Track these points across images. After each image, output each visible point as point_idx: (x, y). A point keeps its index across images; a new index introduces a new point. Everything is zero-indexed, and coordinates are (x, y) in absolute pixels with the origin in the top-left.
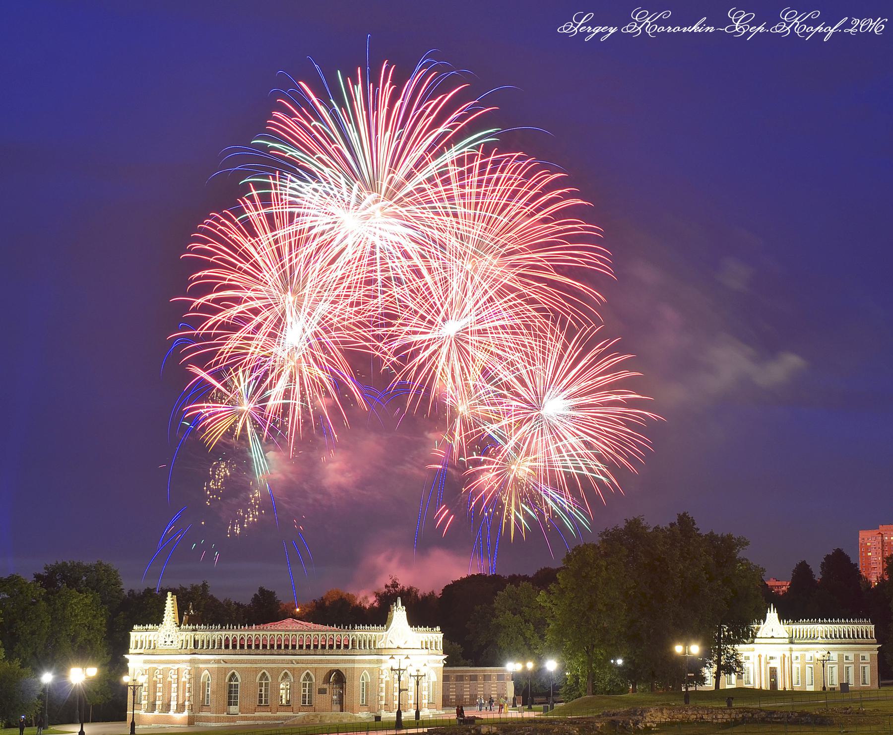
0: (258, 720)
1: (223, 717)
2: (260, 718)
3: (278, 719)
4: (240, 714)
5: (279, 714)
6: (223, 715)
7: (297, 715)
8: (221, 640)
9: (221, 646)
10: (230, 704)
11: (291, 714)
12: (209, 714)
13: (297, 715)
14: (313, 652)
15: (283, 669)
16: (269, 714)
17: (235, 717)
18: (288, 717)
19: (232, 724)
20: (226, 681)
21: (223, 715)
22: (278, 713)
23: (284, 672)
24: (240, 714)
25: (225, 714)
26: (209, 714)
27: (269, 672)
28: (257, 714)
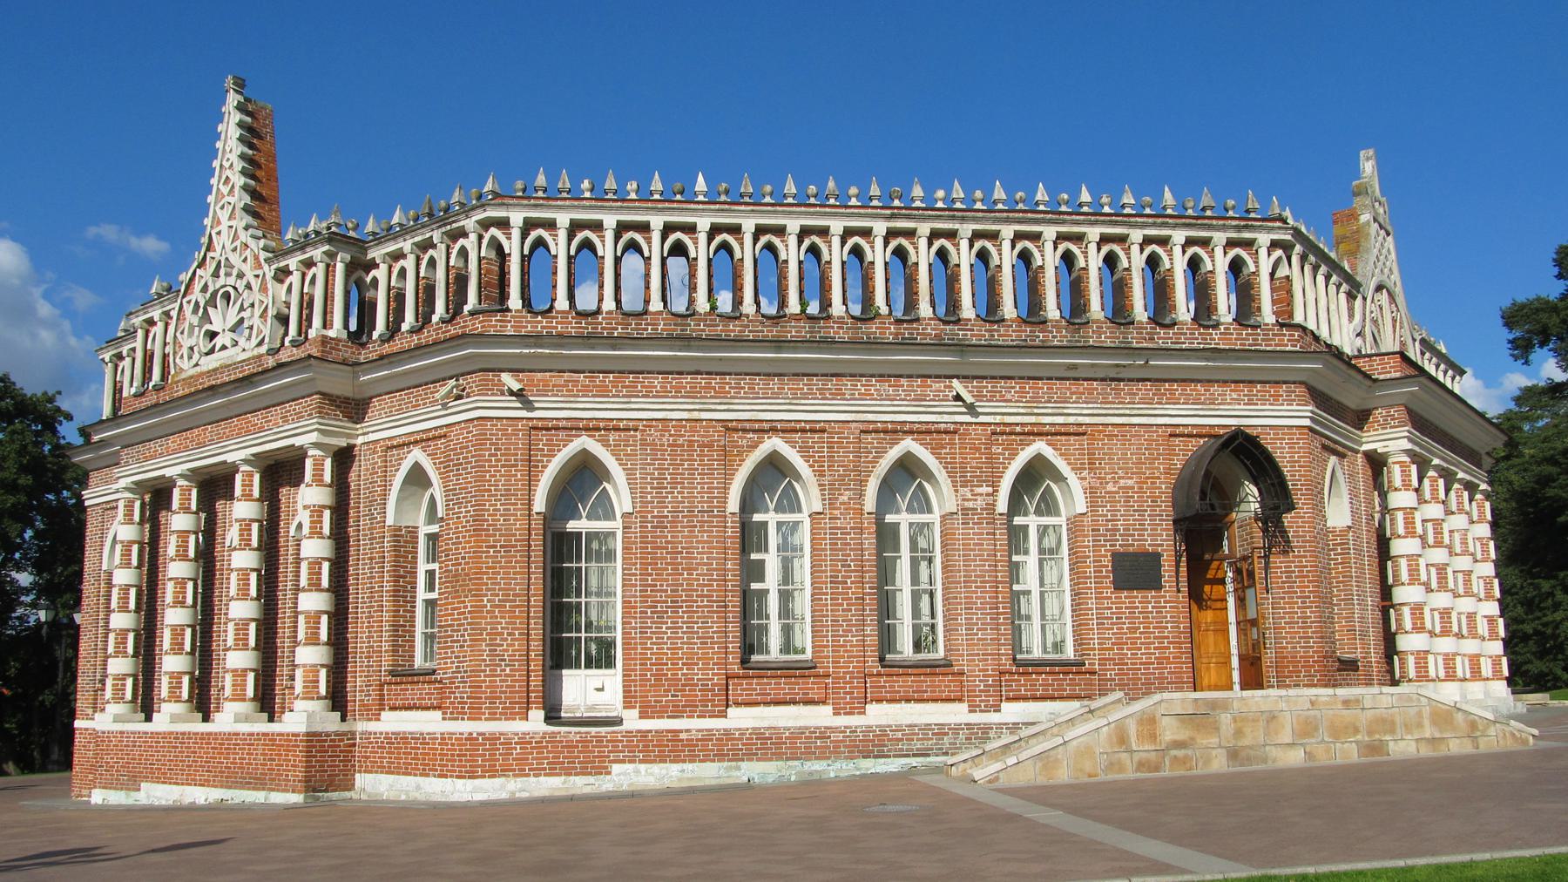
0: (750, 756)
1: (524, 740)
2: (765, 744)
3: (875, 744)
4: (633, 721)
5: (879, 715)
6: (518, 726)
7: (993, 718)
8: (502, 255)
9: (504, 296)
10: (559, 655)
11: (956, 713)
12: (428, 722)
13: (993, 718)
14: (1059, 337)
15: (895, 432)
16: (821, 716)
17: (599, 739)
18: (941, 731)
19: (580, 784)
20: (539, 505)
21: (518, 726)
22: (872, 708)
23: (894, 453)
24: (633, 721)
25: (536, 721)
26: (428, 722)
27: (804, 451)
28: (741, 718)
